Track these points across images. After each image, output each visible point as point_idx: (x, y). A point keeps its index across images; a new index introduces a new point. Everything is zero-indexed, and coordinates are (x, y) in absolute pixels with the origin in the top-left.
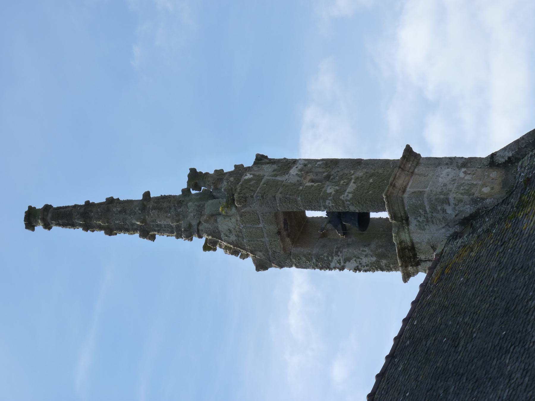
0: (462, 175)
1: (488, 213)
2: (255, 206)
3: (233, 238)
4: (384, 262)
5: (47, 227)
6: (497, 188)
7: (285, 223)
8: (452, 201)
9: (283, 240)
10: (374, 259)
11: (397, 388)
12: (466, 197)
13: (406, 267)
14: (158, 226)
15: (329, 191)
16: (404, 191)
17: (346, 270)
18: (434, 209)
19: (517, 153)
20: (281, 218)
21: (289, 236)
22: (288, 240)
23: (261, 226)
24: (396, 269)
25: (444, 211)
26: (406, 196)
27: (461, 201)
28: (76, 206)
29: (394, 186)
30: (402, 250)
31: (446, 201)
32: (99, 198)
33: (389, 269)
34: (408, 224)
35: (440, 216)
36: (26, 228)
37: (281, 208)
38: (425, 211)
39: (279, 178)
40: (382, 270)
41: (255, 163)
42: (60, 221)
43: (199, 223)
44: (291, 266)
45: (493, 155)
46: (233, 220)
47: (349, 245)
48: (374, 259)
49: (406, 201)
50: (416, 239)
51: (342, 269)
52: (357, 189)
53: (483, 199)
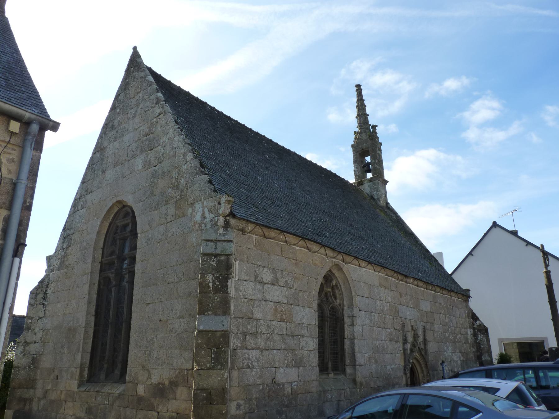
0: (384, 196)
1: (376, 202)
2: (370, 142)
3: (360, 138)
4: (357, 177)
5: (357, 90)
6: (382, 205)
7: (366, 151)
8: (378, 193)
9: (361, 150)
10: (358, 175)
11: (248, 215)
12: (379, 196)
13: (357, 183)
14: (361, 118)
15: (376, 161)
16: (379, 180)
17: (354, 168)
18: (375, 188)
19: (391, 210)
20: (367, 150)
21: (362, 152)
22: (361, 152)
23: (364, 144)
24: (355, 181)
25: (374, 191)
26: (378, 181)
27: (378, 195)
28: (363, 97)
29: (380, 178)
30: (362, 181)
31: (377, 191)
32: (366, 103)
33: (355, 179)
34: (369, 182)
35: (373, 190)
36: (356, 85)
37: (370, 149)
38: (374, 186)
39: (377, 148)
40: (355, 177)
41: (380, 142)
42: (359, 93)
43: (363, 129)
44: (353, 154)
45: (389, 203)
46: (365, 137)
47: (361, 168)
48: (358, 175)
49: (376, 181)
50: (365, 185)
51: (354, 167)
52: (377, 168)
53: (379, 201)
